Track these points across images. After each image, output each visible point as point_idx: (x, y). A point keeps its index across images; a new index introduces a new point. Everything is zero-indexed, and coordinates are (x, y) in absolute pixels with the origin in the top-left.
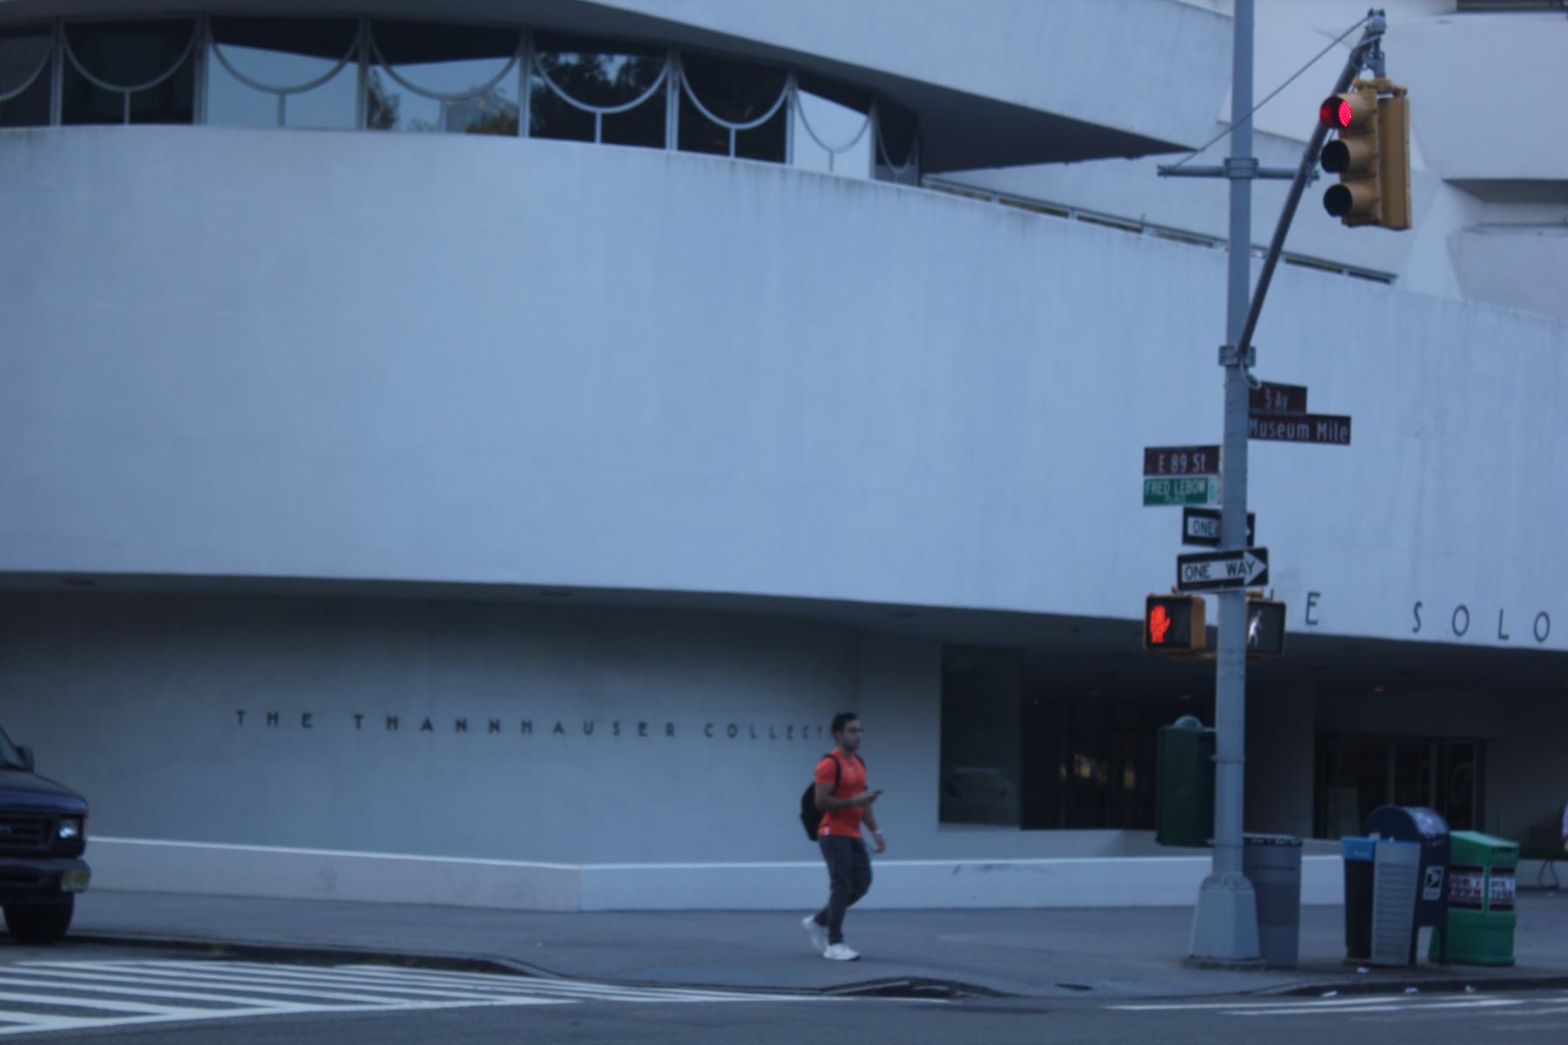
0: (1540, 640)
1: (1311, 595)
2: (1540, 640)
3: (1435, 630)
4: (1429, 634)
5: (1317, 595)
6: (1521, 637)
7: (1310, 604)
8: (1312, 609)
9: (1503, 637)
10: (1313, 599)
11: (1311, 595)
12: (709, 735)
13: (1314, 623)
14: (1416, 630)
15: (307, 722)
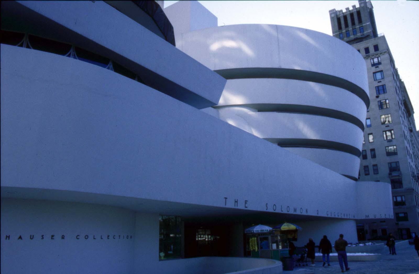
0: (288, 212)
1: (246, 201)
2: (288, 212)
3: (270, 210)
5: (247, 201)
6: (285, 212)
7: (246, 203)
8: (246, 204)
9: (282, 211)
10: (246, 202)
12: (114, 238)
13: (246, 207)
14: (267, 209)
15: (53, 238)
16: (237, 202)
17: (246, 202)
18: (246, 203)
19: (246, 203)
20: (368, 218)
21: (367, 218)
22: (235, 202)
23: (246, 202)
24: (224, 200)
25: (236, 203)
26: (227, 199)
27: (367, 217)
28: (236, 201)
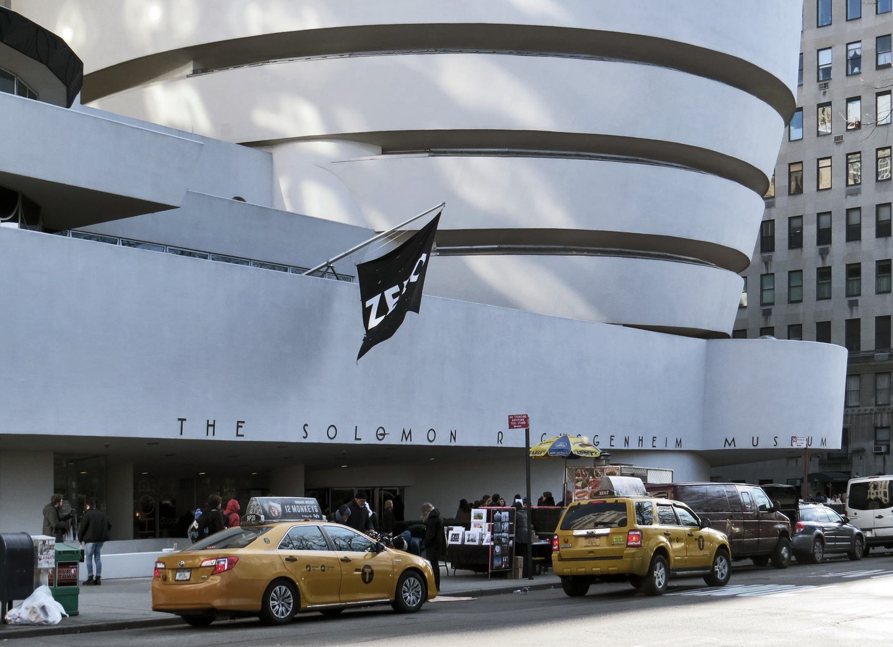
1: (238, 422)
4: (313, 439)
6: (368, 438)
7: (238, 427)
10: (240, 424)
11: (238, 422)
16: (213, 426)
17: (239, 425)
18: (241, 427)
19: (241, 427)
20: (732, 447)
21: (727, 447)
22: (208, 425)
23: (239, 425)
24: (180, 422)
25: (211, 429)
26: (184, 422)
27: (730, 445)
28: (211, 423)
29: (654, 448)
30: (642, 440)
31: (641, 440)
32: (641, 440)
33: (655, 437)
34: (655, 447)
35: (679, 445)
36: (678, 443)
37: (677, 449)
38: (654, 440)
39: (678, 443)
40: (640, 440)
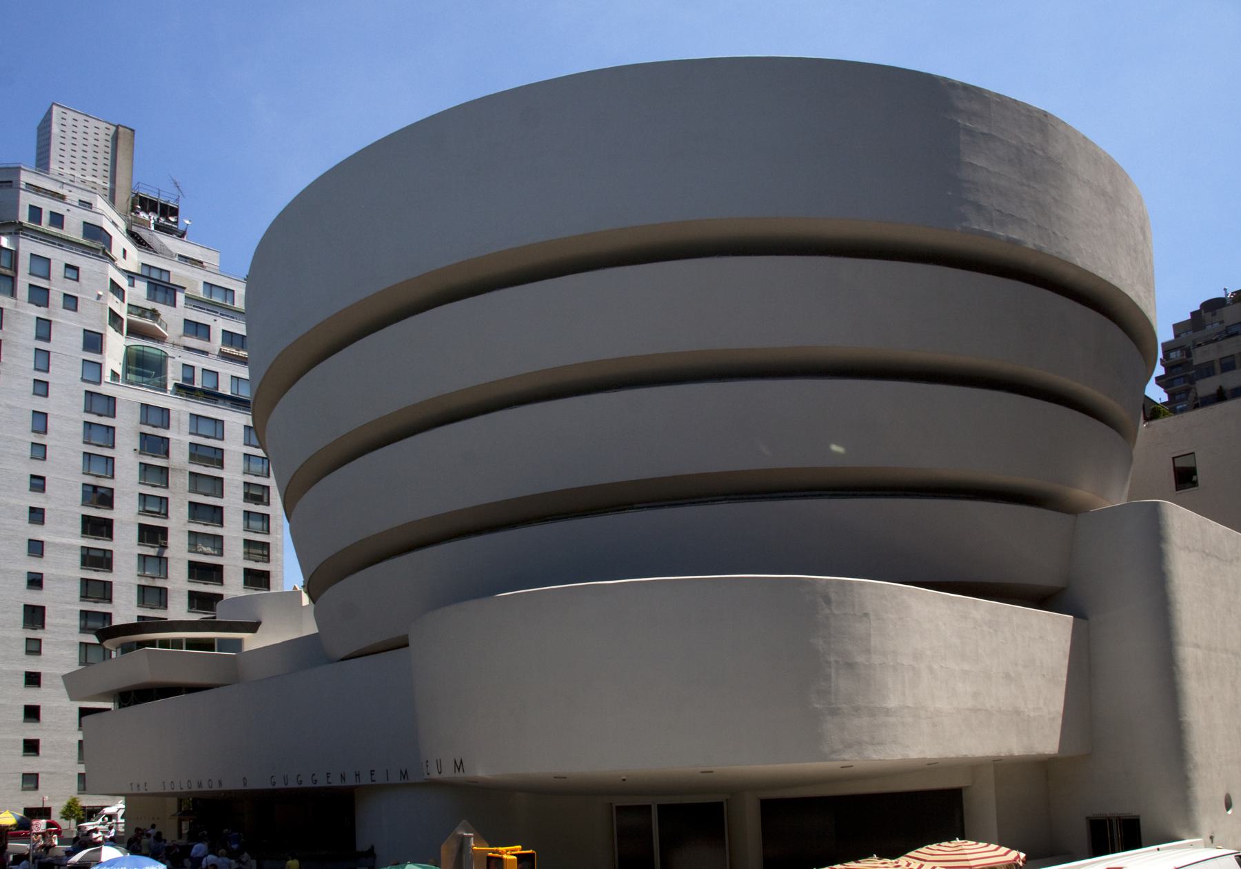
29: (373, 783)
30: (359, 775)
31: (357, 775)
32: (357, 775)
33: (374, 771)
34: (374, 781)
35: (404, 778)
36: (404, 775)
37: (403, 781)
38: (372, 774)
39: (404, 775)
40: (356, 775)
